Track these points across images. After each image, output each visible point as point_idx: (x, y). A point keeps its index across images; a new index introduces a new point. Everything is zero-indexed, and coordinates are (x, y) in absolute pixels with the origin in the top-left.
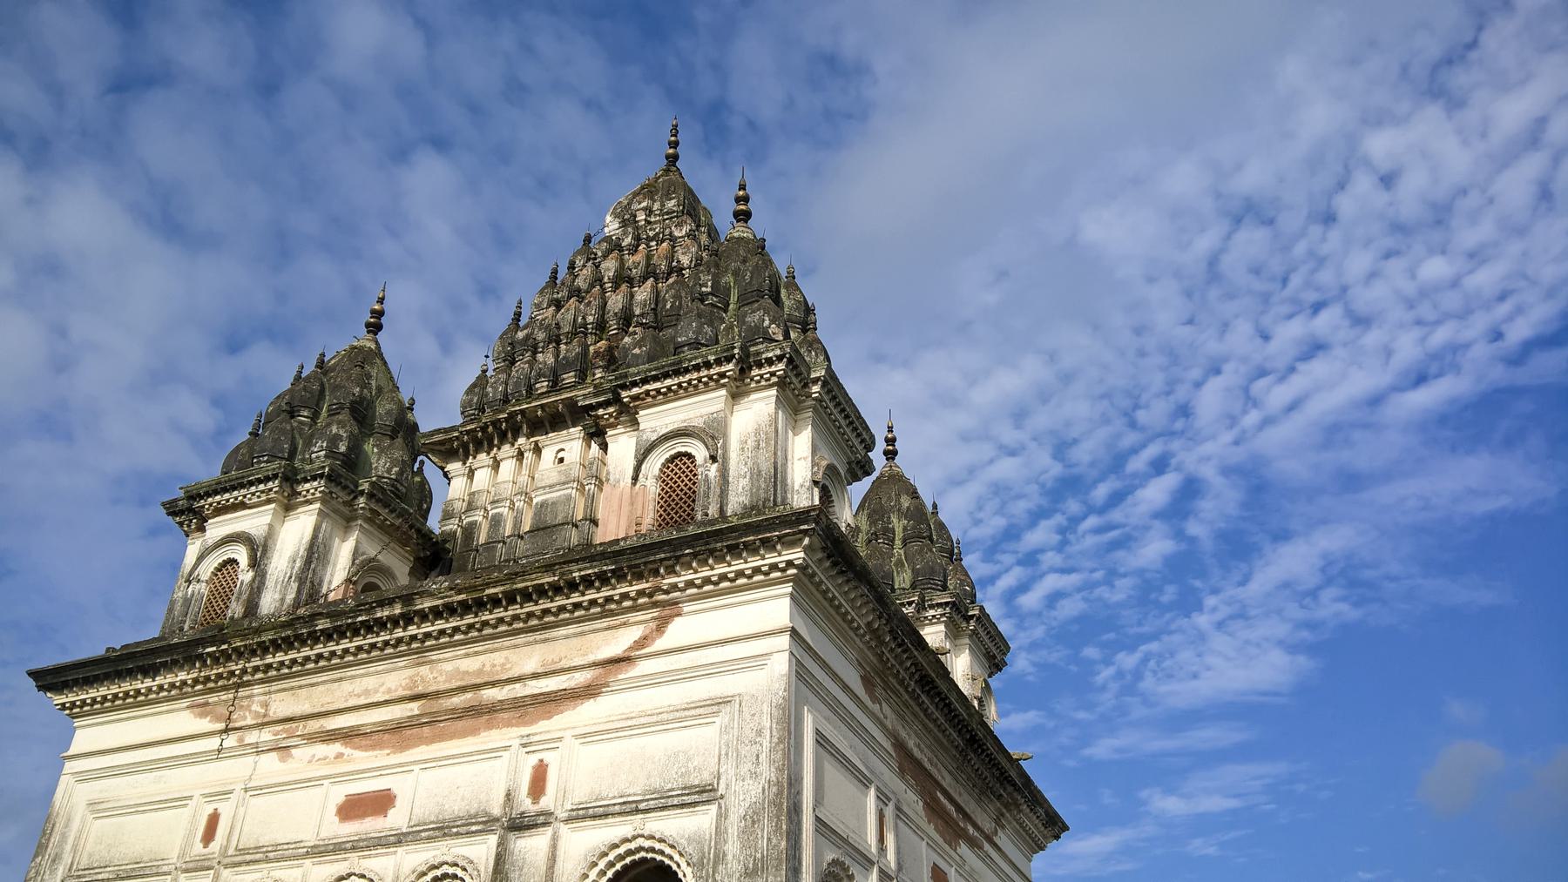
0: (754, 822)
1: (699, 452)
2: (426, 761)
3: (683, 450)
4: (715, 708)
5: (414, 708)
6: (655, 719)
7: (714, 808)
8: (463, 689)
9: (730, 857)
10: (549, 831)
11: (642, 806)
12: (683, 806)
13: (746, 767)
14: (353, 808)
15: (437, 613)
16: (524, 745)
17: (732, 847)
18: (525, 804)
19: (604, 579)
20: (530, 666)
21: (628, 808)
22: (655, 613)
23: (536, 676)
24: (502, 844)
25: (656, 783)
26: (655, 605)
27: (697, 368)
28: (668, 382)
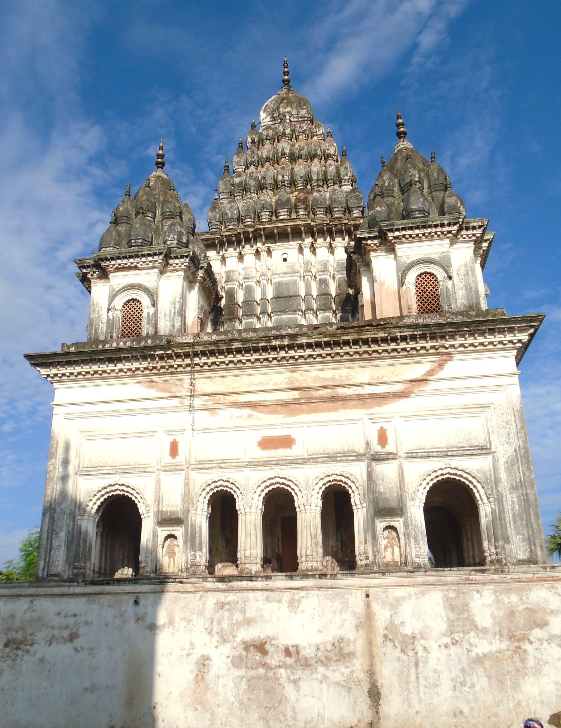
0: (512, 465)
1: (440, 274)
2: (310, 423)
3: (428, 271)
4: (482, 409)
5: (296, 394)
6: (447, 412)
7: (490, 457)
8: (325, 387)
9: (503, 480)
10: (395, 463)
11: (449, 454)
12: (472, 455)
13: (503, 439)
14: (267, 443)
15: (309, 346)
16: (370, 419)
17: (503, 476)
18: (376, 448)
19: (413, 338)
20: (366, 380)
21: (441, 454)
22: (437, 358)
23: (370, 384)
24: (369, 467)
25: (453, 443)
26: (438, 354)
27: (436, 226)
28: (417, 231)
